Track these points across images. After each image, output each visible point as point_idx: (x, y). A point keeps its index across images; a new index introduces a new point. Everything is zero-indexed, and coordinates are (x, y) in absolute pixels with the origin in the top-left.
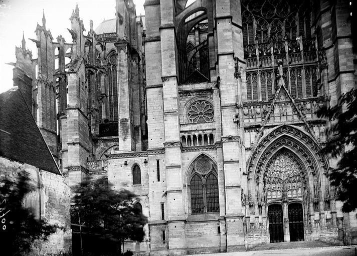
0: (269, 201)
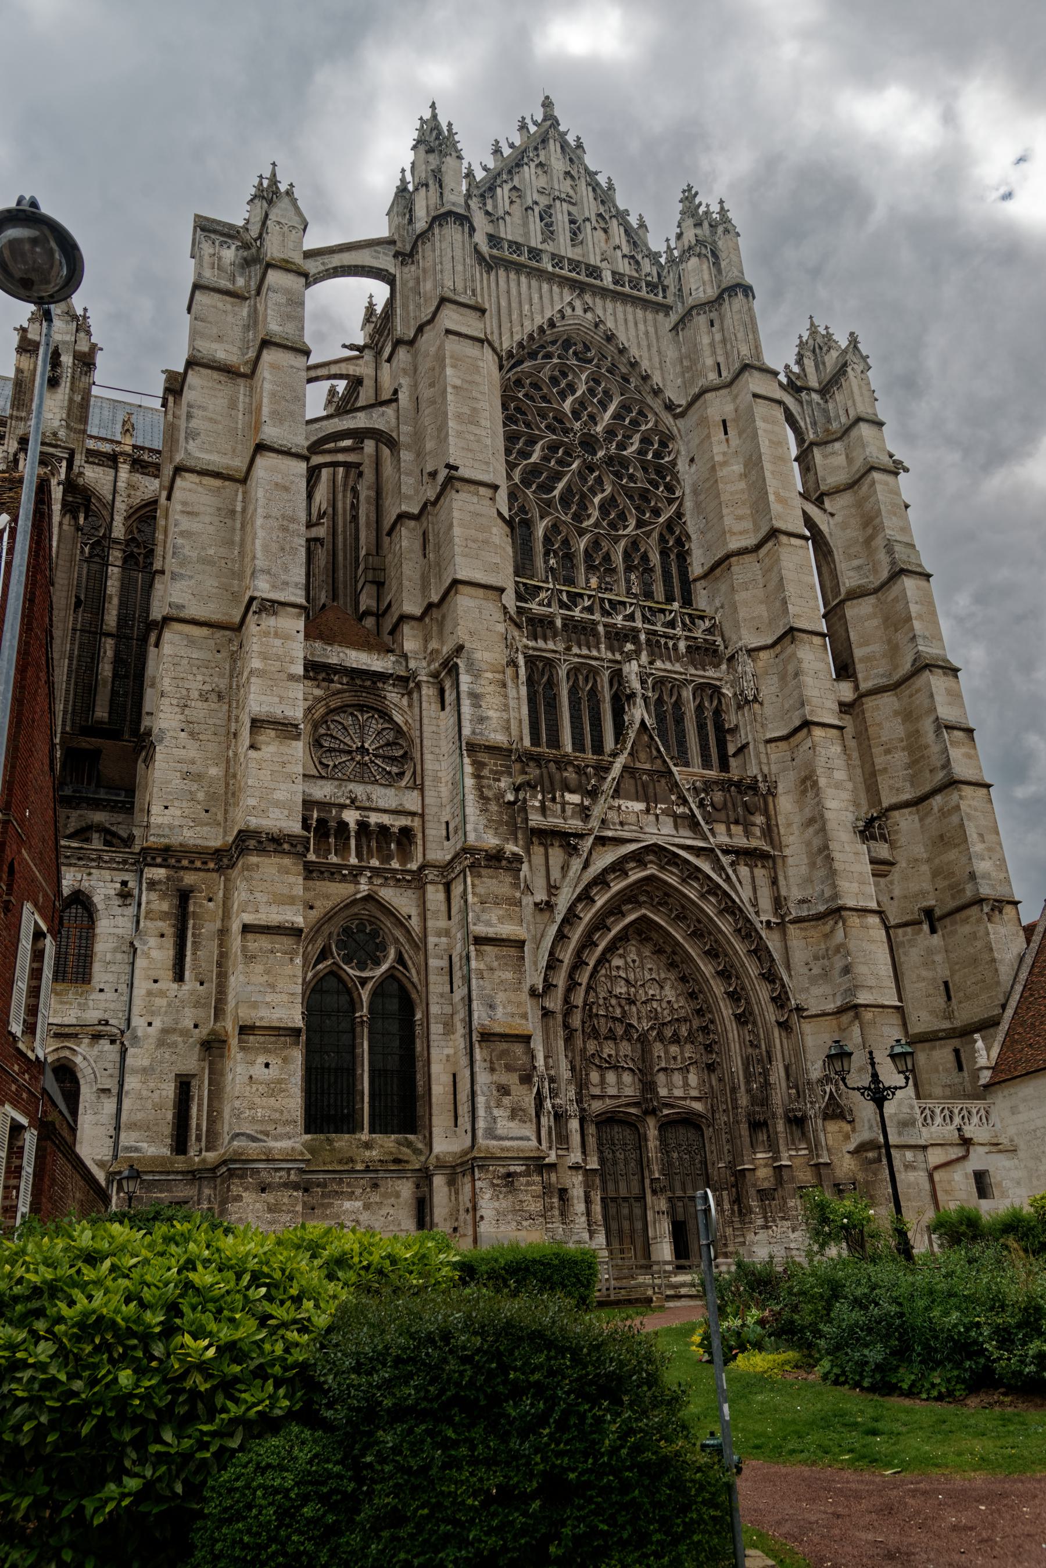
0: (597, 1106)
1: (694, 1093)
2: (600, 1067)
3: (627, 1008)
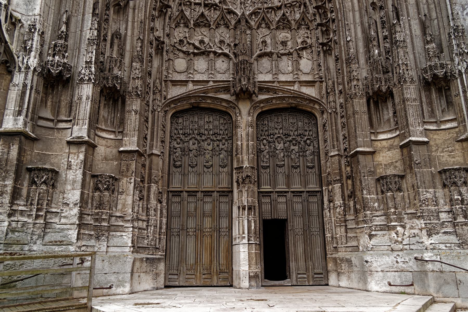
1: (309, 78)
2: (187, 53)
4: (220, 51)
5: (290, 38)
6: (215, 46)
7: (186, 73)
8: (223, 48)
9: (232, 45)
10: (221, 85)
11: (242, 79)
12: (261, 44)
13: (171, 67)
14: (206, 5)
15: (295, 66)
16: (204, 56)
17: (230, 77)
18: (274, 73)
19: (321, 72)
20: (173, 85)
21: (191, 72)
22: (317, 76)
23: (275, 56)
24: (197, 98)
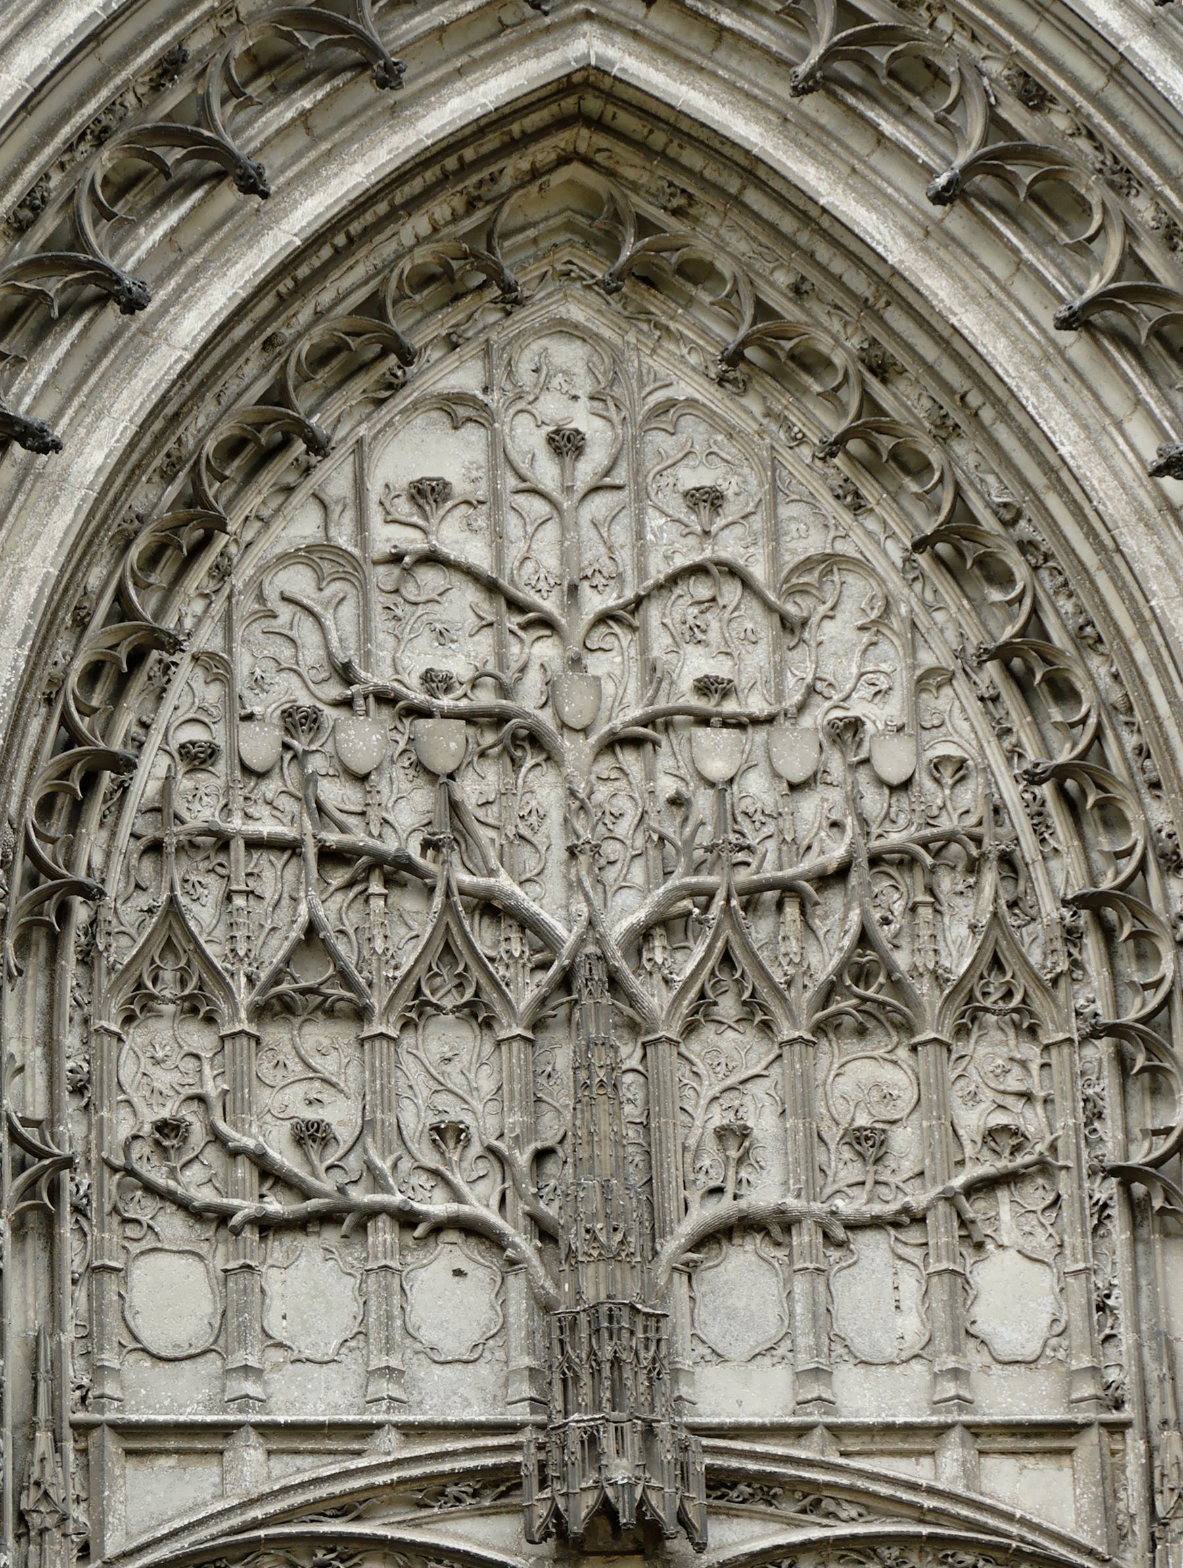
3: (469, 790)
4: (438, 1206)
5: (908, 1096)
6: (406, 1165)
7: (212, 1364)
8: (458, 1179)
9: (522, 1158)
10: (454, 1454)
11: (608, 1442)
12: (711, 1144)
13: (112, 1320)
14: (330, 857)
15: (942, 1316)
16: (331, 1236)
17: (514, 1393)
18: (805, 1362)
19: (1110, 1349)
20: (129, 1453)
21: (252, 1362)
22: (1087, 1389)
23: (804, 1237)
24: (300, 1549)
